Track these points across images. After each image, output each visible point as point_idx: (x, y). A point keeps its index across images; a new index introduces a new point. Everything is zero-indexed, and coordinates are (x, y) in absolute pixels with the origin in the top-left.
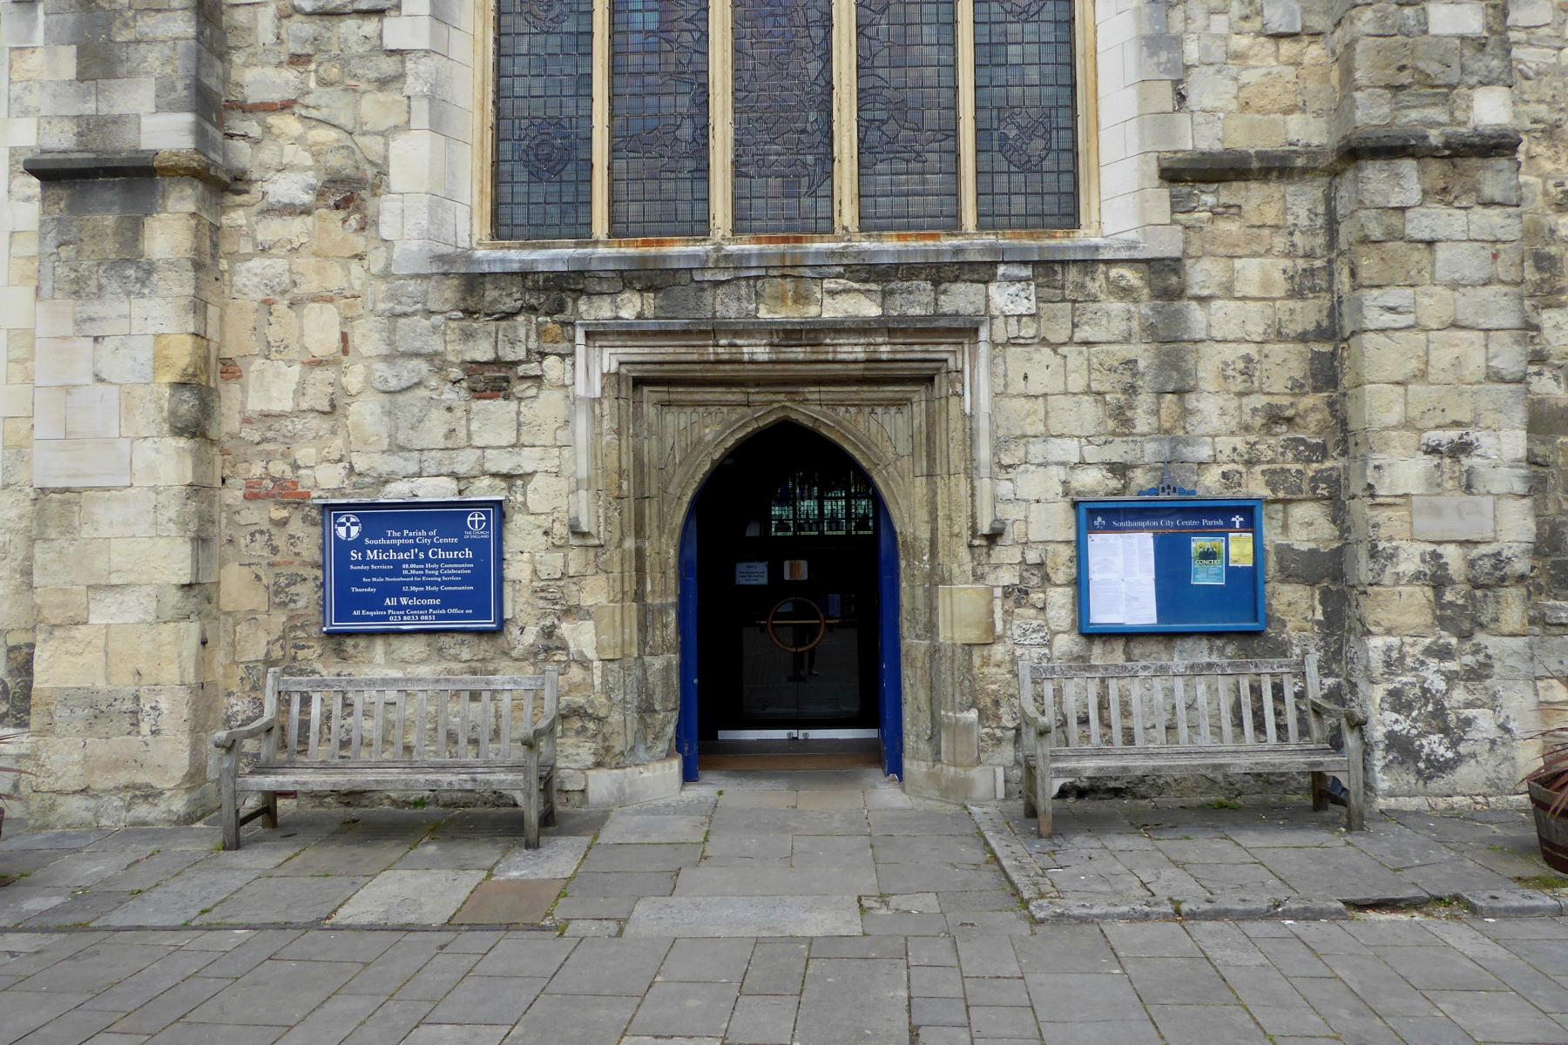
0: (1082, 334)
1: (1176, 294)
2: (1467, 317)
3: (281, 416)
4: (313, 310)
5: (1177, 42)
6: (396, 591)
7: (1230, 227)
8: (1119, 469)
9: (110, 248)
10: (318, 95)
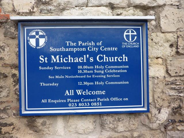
6: (74, 84)
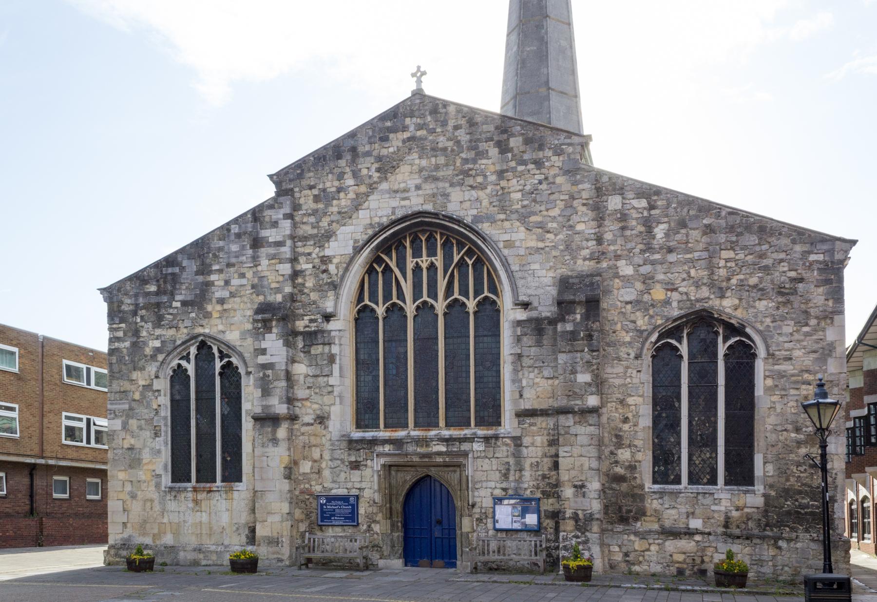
0: (497, 455)
1: (521, 445)
2: (584, 454)
3: (307, 474)
4: (313, 448)
5: (521, 381)
6: (334, 516)
7: (535, 428)
8: (504, 490)
9: (270, 436)
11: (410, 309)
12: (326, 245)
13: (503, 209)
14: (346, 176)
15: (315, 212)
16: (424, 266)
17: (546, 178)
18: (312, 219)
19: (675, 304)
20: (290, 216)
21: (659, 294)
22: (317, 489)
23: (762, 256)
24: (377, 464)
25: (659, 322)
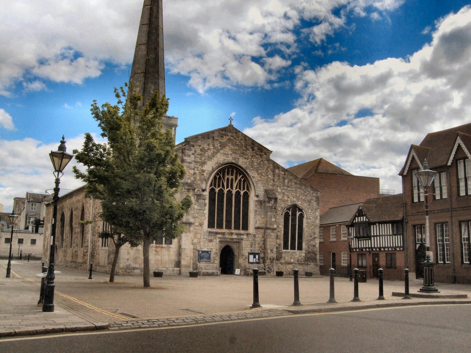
0: (250, 240)
8: (251, 250)
10: (199, 217)
11: (226, 191)
12: (204, 166)
13: (252, 167)
14: (210, 145)
15: (200, 154)
16: (230, 178)
17: (262, 161)
18: (199, 156)
19: (289, 201)
20: (193, 154)
21: (286, 198)
22: (199, 248)
23: (305, 192)
24: (218, 240)
25: (286, 206)
